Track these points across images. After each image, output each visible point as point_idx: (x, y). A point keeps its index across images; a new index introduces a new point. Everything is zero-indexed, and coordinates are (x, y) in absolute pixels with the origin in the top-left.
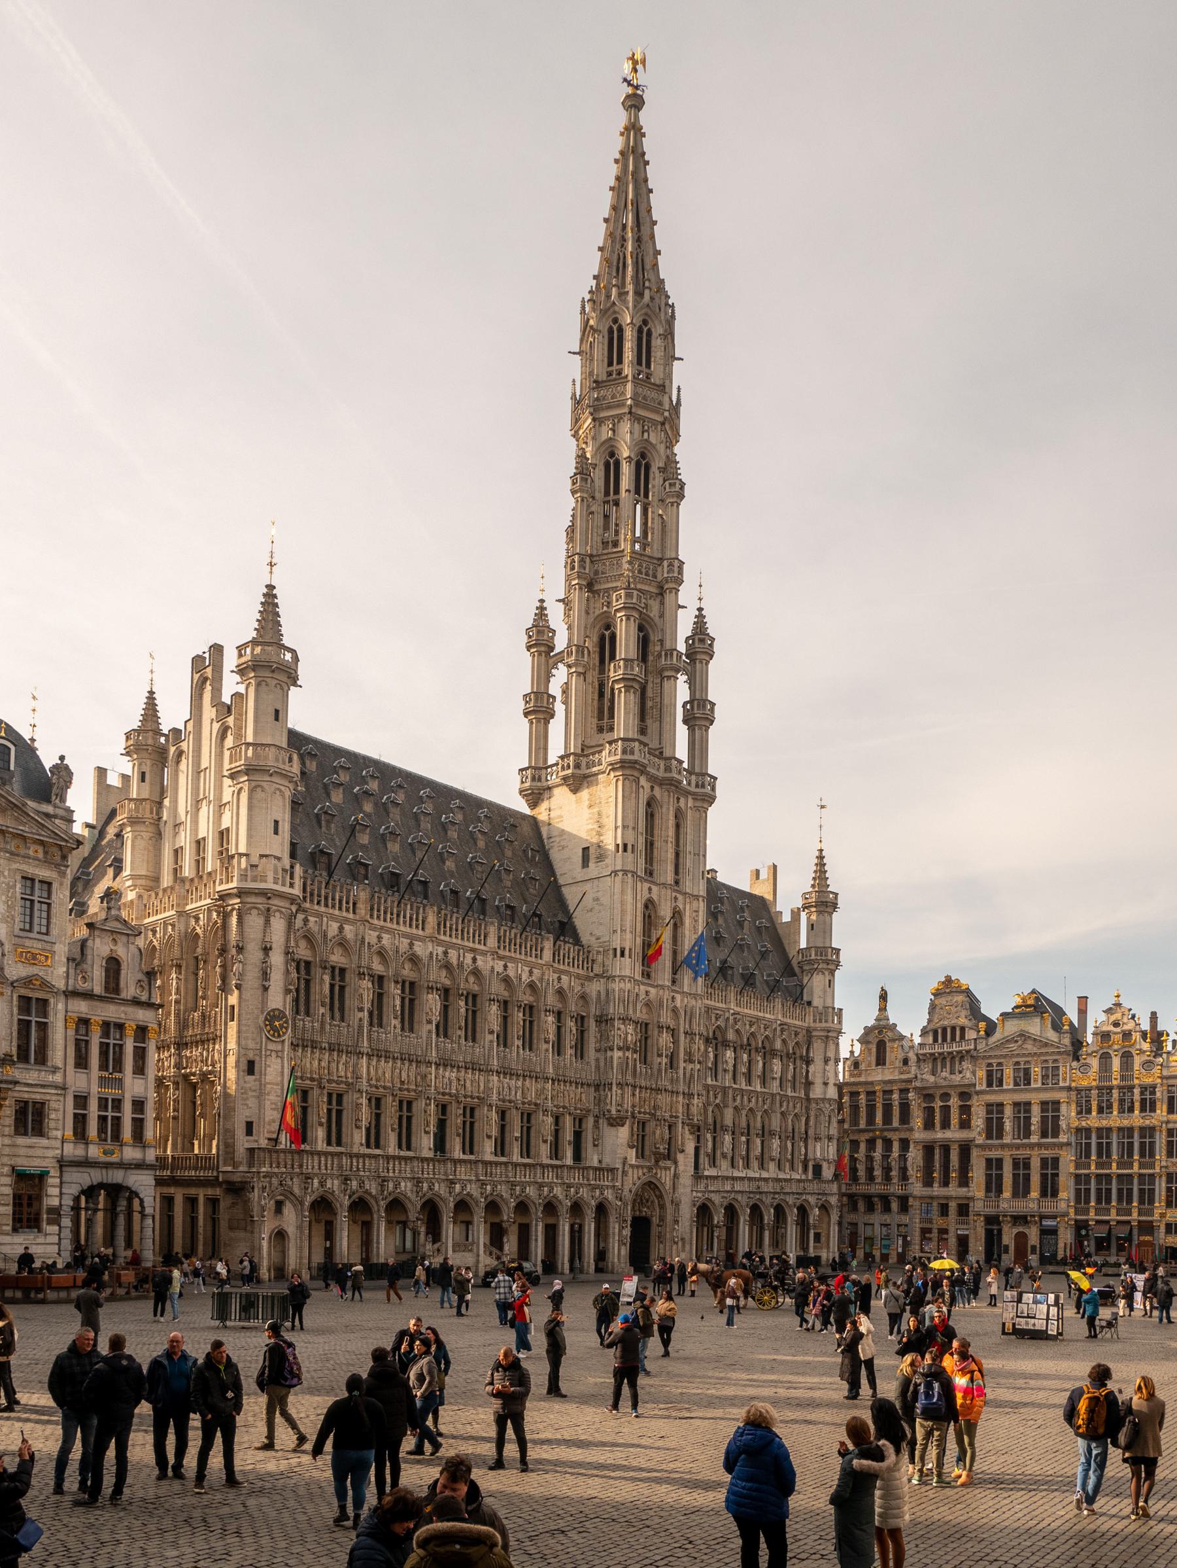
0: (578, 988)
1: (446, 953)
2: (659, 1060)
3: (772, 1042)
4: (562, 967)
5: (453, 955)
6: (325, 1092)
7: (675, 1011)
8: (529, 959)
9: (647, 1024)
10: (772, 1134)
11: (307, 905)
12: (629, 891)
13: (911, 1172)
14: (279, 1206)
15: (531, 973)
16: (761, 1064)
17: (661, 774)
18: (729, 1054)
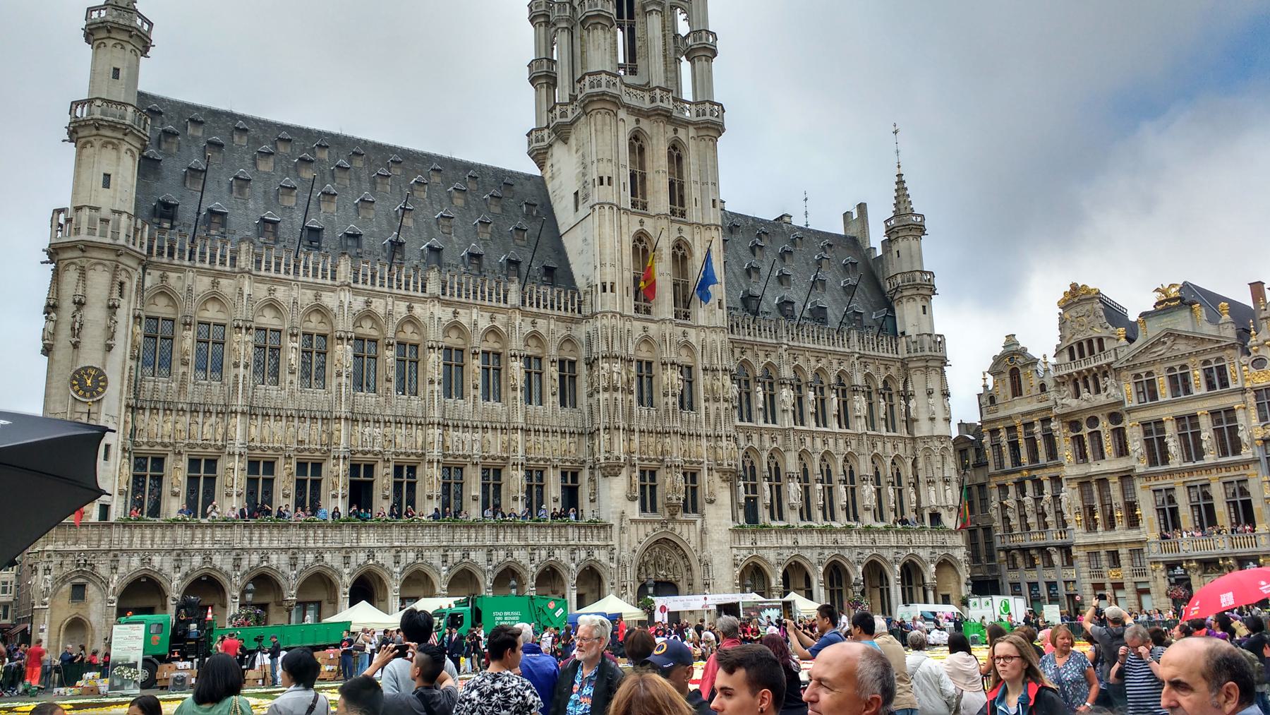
0: (562, 332)
1: (368, 303)
2: (666, 399)
3: (850, 377)
4: (535, 309)
5: (378, 306)
6: (185, 459)
7: (687, 345)
8: (487, 303)
9: (649, 364)
10: (864, 479)
11: (154, 259)
12: (607, 223)
13: (1067, 516)
14: (78, 592)
15: (492, 319)
16: (835, 400)
17: (647, 105)
18: (786, 396)
